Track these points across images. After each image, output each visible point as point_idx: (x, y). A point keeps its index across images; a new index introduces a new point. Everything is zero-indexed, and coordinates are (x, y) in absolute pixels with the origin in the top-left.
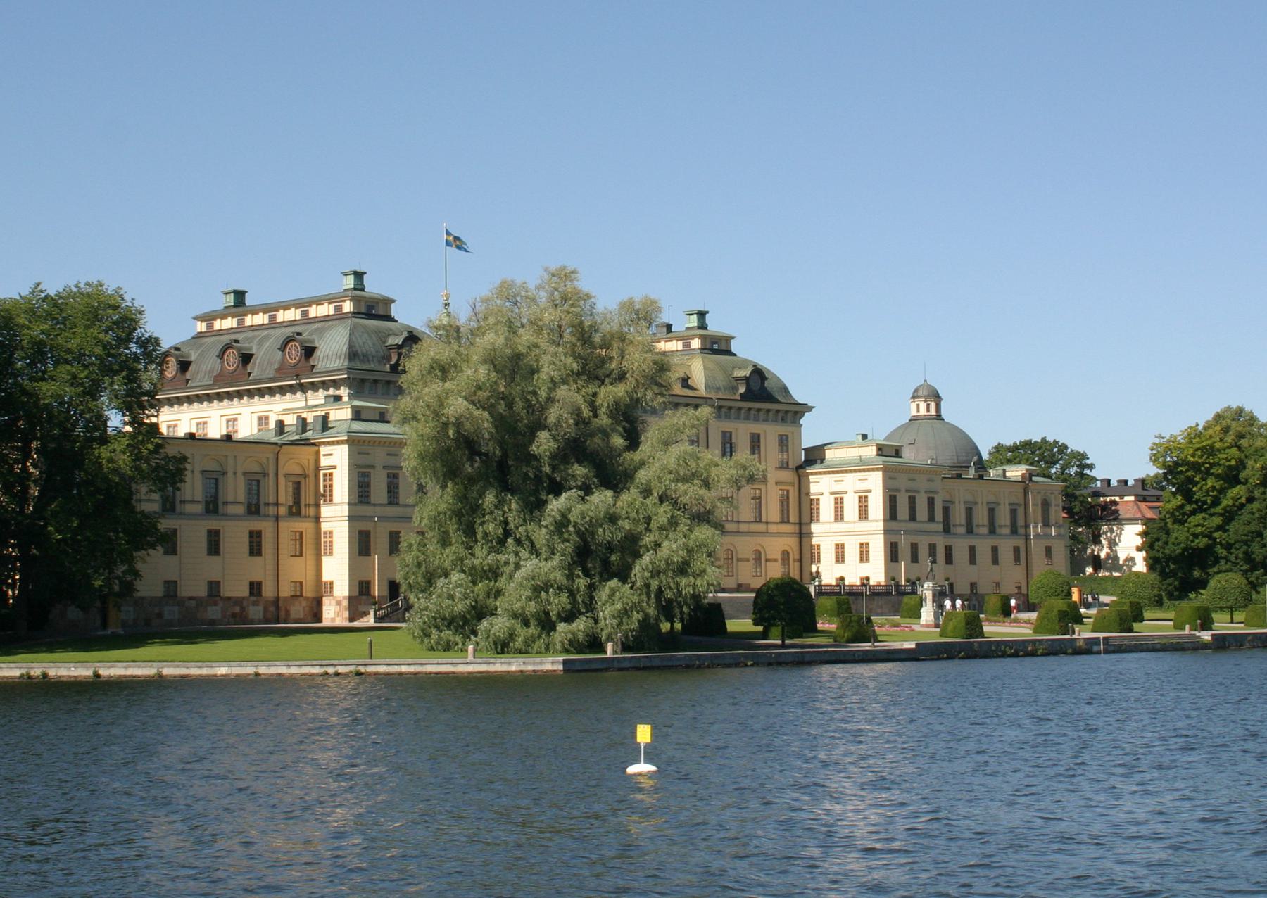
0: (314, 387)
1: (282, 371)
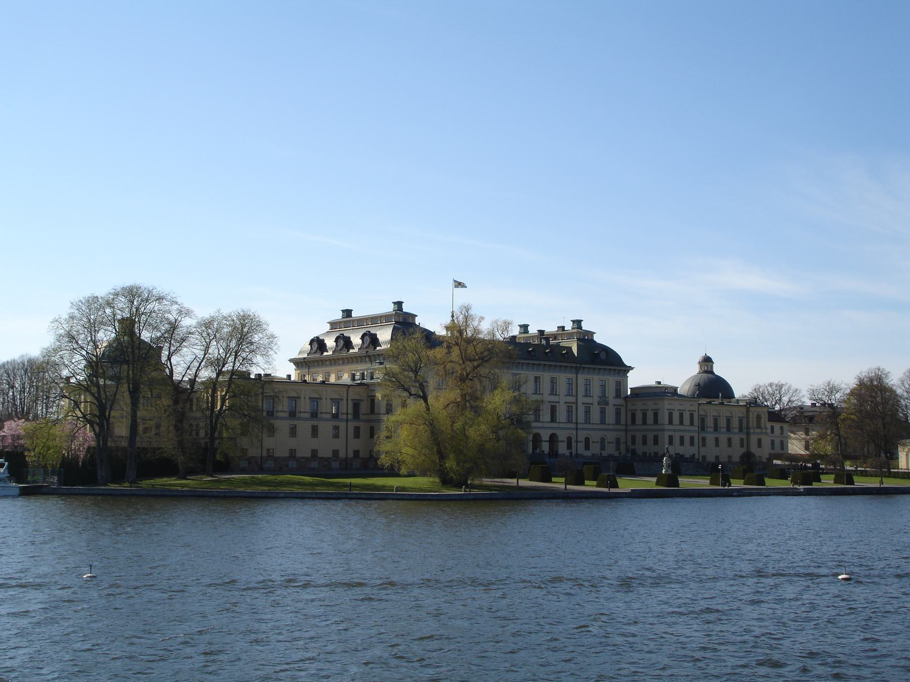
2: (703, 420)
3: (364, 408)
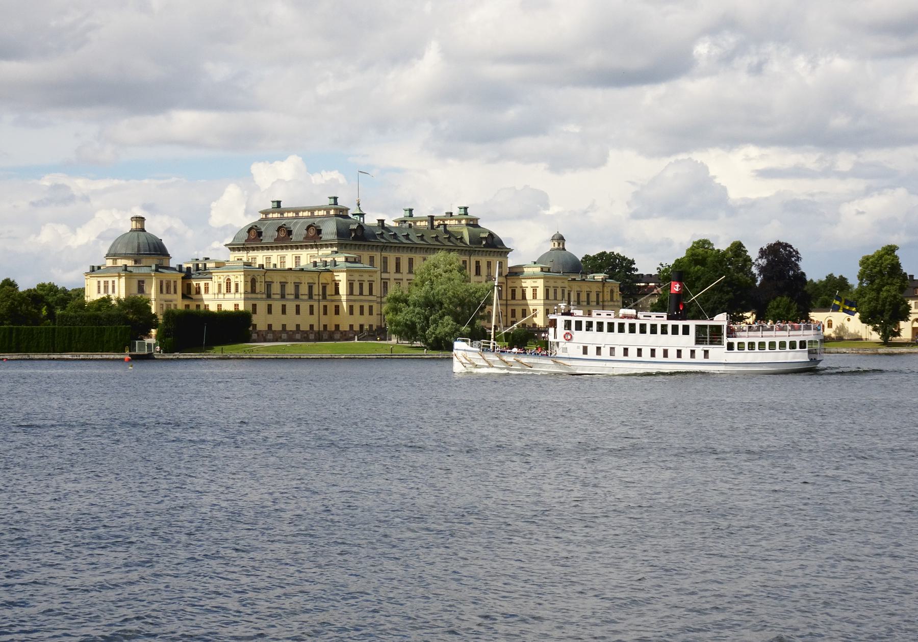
0: (322, 246)
1: (307, 238)
3: (330, 290)
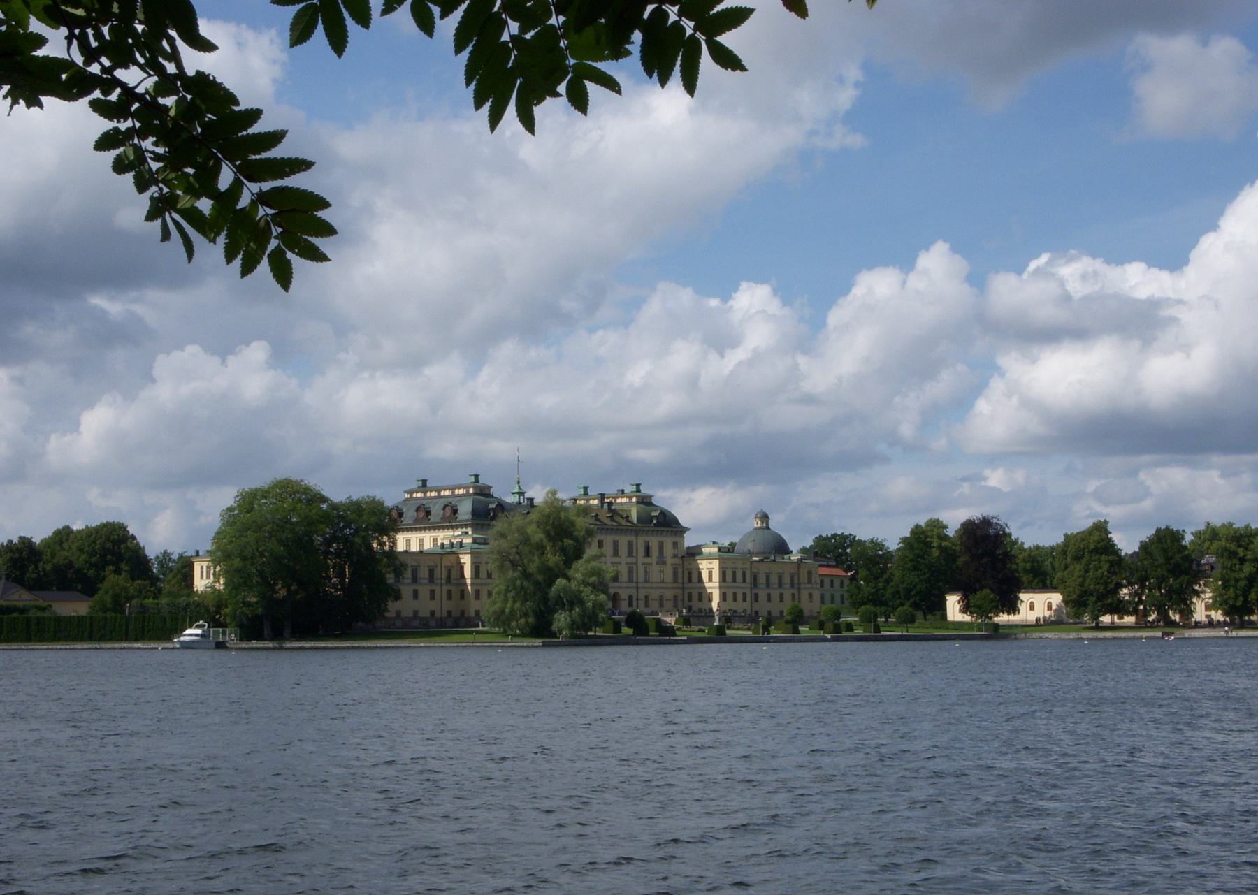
0: (457, 527)
1: (444, 519)
2: (755, 578)
3: (454, 574)
